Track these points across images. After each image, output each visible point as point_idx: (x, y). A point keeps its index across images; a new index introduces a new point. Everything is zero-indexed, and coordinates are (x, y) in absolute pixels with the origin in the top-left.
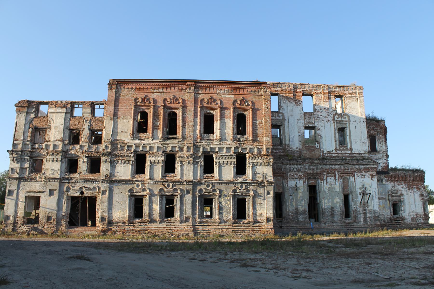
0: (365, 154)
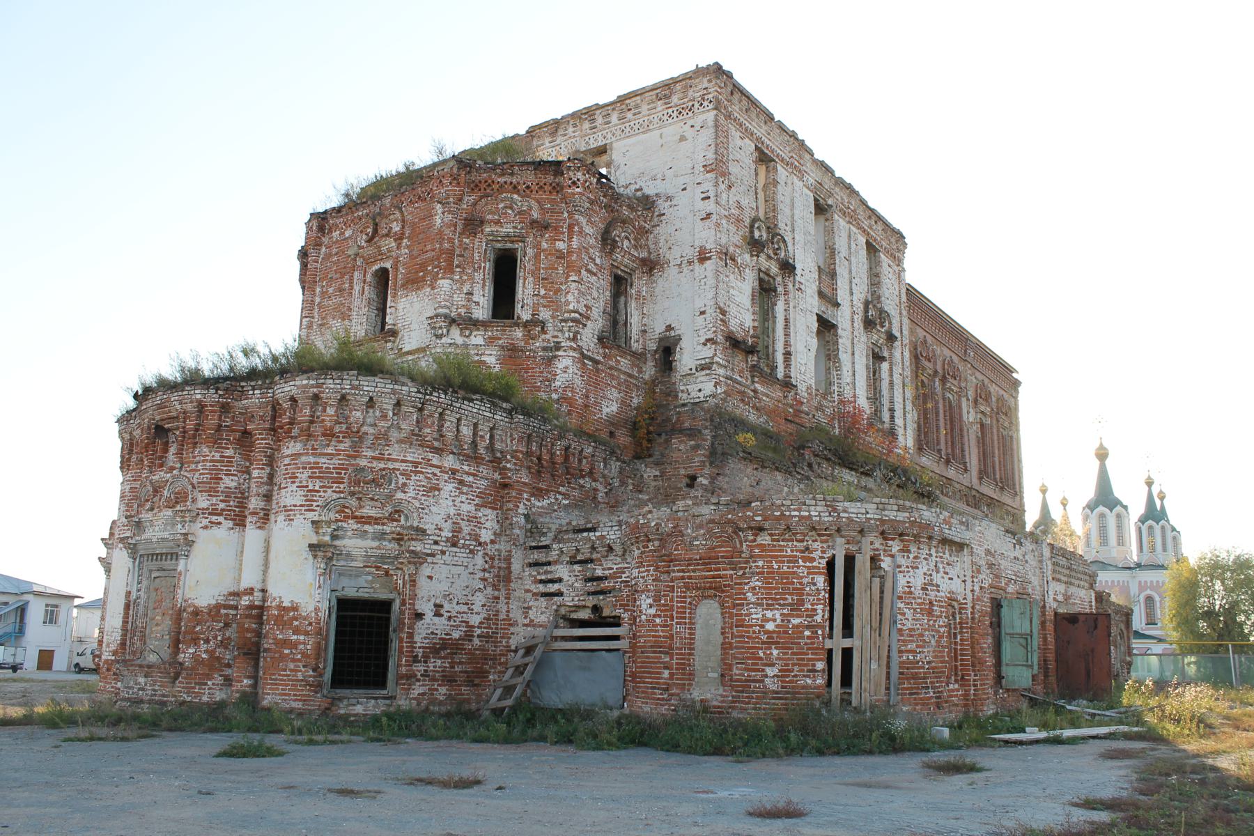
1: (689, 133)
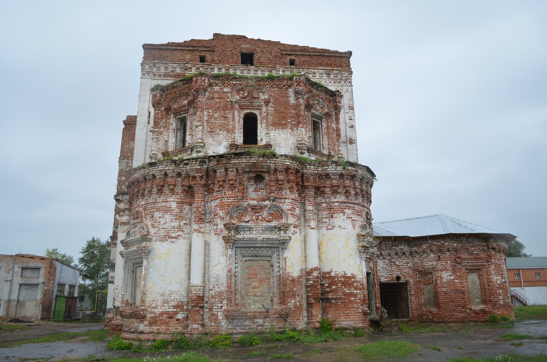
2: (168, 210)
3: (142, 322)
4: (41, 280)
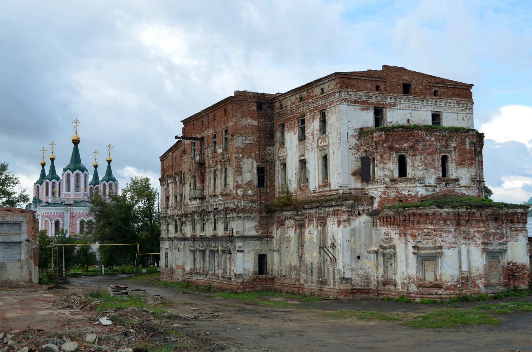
0: (340, 189)
1: (465, 118)
2: (449, 233)
3: (440, 289)
4: (24, 237)
